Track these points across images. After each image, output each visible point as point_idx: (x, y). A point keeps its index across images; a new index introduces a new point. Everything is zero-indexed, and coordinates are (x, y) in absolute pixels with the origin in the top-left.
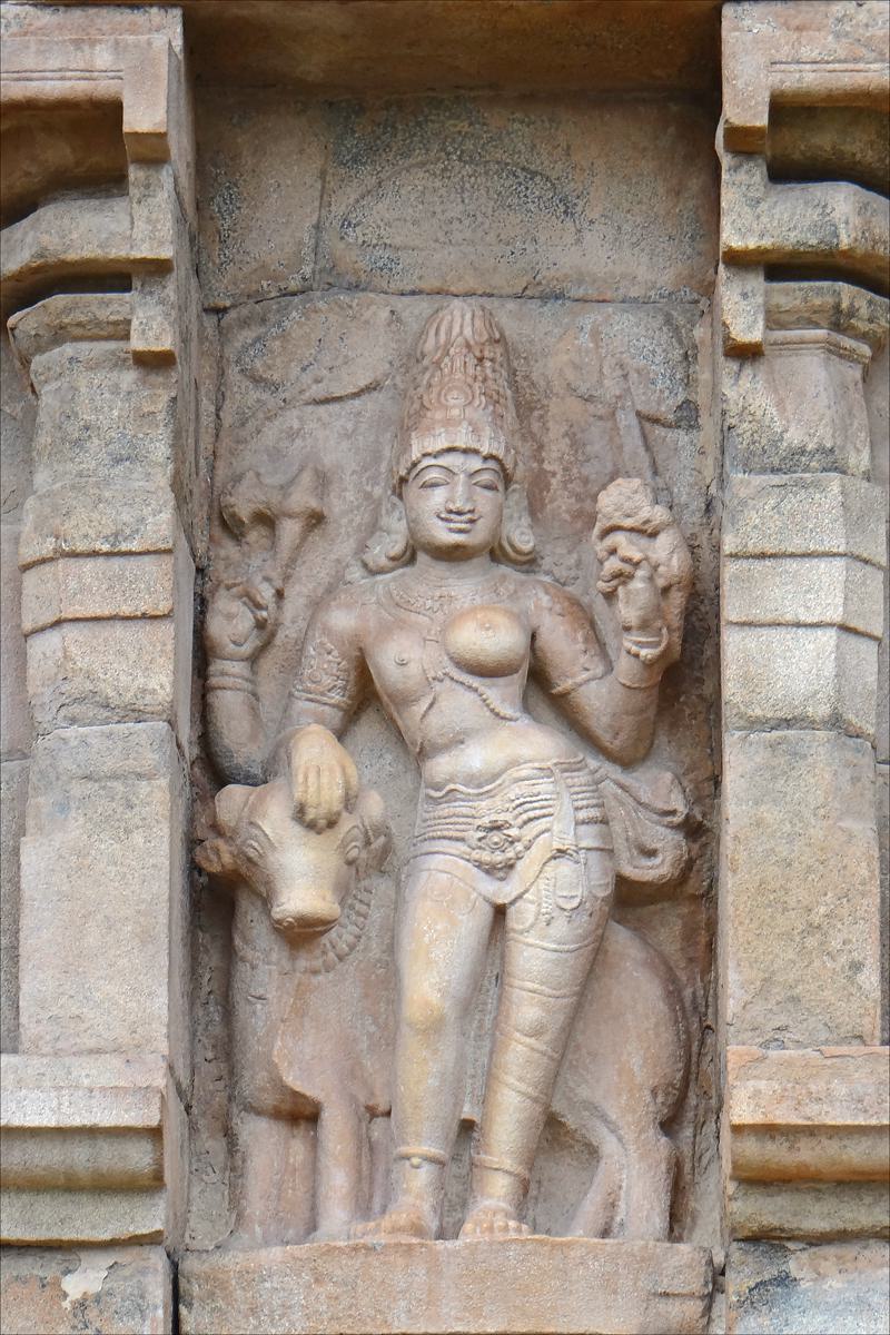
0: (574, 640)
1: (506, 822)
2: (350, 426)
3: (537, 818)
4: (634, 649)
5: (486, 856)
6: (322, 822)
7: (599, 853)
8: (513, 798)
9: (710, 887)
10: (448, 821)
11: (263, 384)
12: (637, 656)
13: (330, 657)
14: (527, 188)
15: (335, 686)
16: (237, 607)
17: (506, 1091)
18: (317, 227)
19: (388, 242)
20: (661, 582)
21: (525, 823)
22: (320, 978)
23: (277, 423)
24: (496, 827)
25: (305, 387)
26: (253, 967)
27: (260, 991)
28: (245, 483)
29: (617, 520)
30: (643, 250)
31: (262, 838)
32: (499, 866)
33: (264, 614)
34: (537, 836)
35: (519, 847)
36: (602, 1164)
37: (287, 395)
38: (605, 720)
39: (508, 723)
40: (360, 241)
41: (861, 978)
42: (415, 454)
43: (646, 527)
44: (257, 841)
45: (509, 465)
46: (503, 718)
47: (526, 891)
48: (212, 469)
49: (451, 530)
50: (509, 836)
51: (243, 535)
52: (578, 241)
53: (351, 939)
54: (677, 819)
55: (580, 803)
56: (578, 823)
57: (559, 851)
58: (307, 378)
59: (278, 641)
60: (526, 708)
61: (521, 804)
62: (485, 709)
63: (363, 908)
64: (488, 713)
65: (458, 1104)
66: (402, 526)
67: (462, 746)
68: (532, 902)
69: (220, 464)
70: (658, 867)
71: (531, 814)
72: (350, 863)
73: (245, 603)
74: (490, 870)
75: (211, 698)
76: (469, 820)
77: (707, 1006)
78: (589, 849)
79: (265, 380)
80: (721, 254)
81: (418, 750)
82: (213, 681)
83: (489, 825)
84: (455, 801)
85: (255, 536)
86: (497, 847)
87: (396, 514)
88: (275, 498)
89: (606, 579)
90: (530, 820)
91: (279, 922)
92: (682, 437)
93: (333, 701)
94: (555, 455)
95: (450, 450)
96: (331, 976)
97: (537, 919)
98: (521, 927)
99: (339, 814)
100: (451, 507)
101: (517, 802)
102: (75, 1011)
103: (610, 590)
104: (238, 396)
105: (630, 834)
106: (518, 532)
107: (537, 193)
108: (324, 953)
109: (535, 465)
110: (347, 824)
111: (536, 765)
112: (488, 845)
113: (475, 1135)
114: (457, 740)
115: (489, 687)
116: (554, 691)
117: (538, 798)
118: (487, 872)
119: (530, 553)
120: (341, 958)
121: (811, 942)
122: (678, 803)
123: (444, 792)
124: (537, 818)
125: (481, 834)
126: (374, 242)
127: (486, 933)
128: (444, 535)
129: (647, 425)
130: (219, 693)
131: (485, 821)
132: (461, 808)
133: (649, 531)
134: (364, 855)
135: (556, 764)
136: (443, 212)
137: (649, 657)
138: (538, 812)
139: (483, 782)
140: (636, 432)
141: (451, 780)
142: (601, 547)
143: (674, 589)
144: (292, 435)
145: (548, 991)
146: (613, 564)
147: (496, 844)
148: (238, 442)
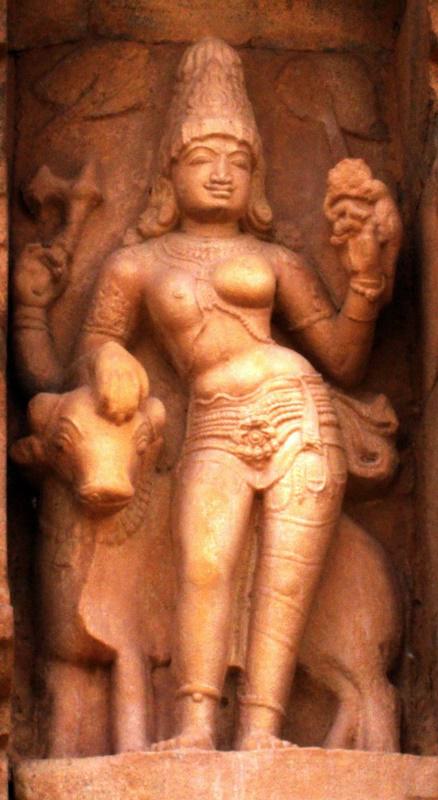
1: (265, 422)
3: (288, 419)
4: (361, 289)
5: (248, 450)
6: (122, 416)
10: (216, 422)
12: (363, 294)
16: (37, 266)
24: (256, 426)
29: (345, 189)
32: (259, 458)
33: (59, 269)
34: (290, 433)
35: (274, 442)
43: (366, 196)
46: (260, 341)
47: (283, 477)
49: (215, 196)
50: (267, 433)
53: (138, 520)
54: (390, 430)
55: (322, 409)
59: (67, 294)
61: (275, 409)
62: (246, 333)
64: (248, 337)
67: (227, 363)
70: (378, 466)
71: (284, 416)
76: (234, 421)
86: (255, 443)
87: (165, 192)
90: (284, 421)
93: (119, 333)
97: (291, 499)
99: (134, 410)
100: (215, 177)
101: (273, 406)
103: (340, 242)
112: (250, 442)
114: (224, 358)
122: (390, 417)
124: (288, 419)
125: (243, 432)
128: (207, 199)
129: (348, 138)
131: (248, 421)
133: (370, 198)
138: (289, 415)
139: (242, 393)
143: (389, 244)
146: (347, 221)
147: (256, 440)
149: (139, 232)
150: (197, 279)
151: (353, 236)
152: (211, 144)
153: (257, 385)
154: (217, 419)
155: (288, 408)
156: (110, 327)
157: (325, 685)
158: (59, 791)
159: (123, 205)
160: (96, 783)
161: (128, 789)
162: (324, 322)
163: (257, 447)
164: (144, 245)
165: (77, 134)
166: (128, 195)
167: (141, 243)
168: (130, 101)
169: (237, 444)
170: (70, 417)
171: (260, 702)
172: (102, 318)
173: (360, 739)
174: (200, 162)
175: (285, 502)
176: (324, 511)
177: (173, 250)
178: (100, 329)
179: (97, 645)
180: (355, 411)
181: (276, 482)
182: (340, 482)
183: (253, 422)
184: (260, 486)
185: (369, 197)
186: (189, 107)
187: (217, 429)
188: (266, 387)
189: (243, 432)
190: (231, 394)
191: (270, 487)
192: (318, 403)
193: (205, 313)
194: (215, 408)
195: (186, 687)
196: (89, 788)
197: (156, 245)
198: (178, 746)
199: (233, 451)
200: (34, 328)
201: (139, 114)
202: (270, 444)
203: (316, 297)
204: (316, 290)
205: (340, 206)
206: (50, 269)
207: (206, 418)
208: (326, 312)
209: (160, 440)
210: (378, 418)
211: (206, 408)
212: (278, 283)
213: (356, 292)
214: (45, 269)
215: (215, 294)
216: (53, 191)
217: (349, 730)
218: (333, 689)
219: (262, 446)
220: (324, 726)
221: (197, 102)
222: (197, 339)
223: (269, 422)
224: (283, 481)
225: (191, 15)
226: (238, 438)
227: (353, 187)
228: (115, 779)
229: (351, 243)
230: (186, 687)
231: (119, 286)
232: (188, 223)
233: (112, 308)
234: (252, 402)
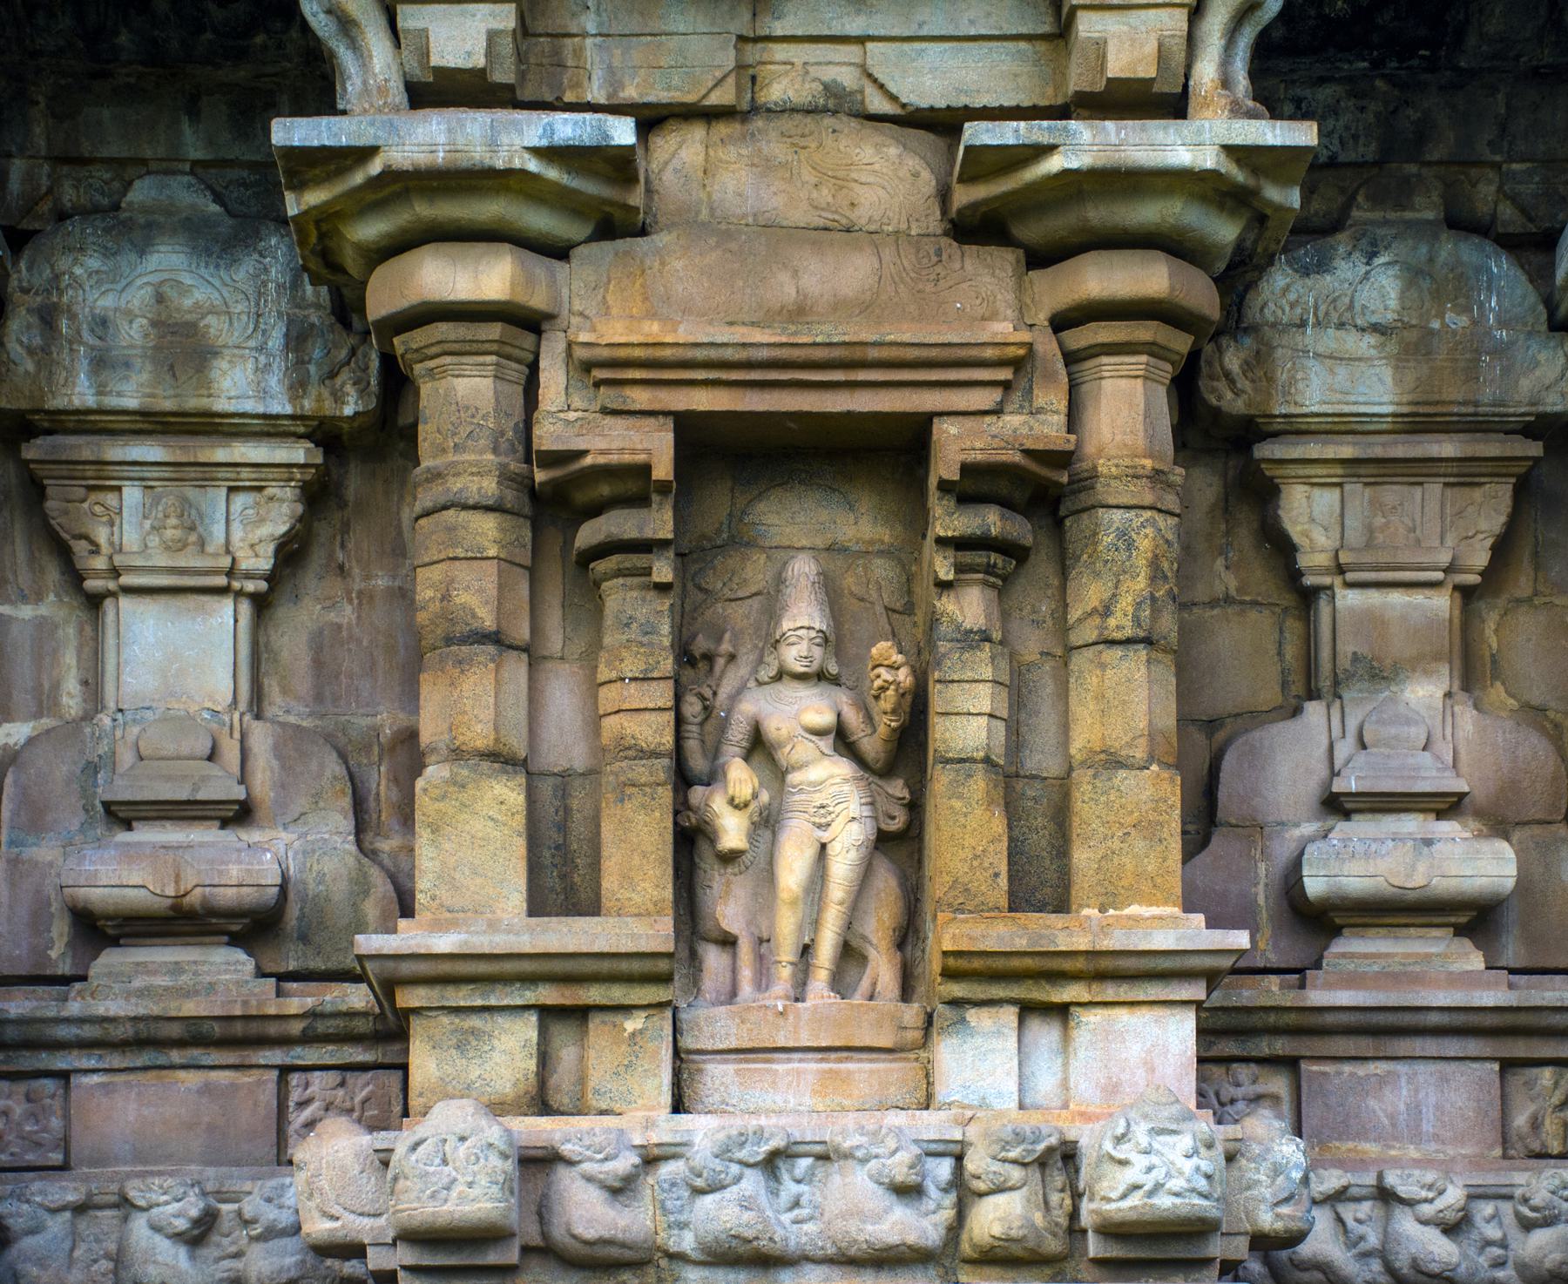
5: (817, 820)
41: (999, 880)
56: (862, 805)
58: (726, 590)
85: (700, 665)
86: (824, 816)
102: (628, 895)
121: (975, 863)
122: (906, 794)
131: (818, 804)
132: (803, 797)
139: (817, 785)
149: (757, 680)
168: (754, 589)
205: (877, 671)
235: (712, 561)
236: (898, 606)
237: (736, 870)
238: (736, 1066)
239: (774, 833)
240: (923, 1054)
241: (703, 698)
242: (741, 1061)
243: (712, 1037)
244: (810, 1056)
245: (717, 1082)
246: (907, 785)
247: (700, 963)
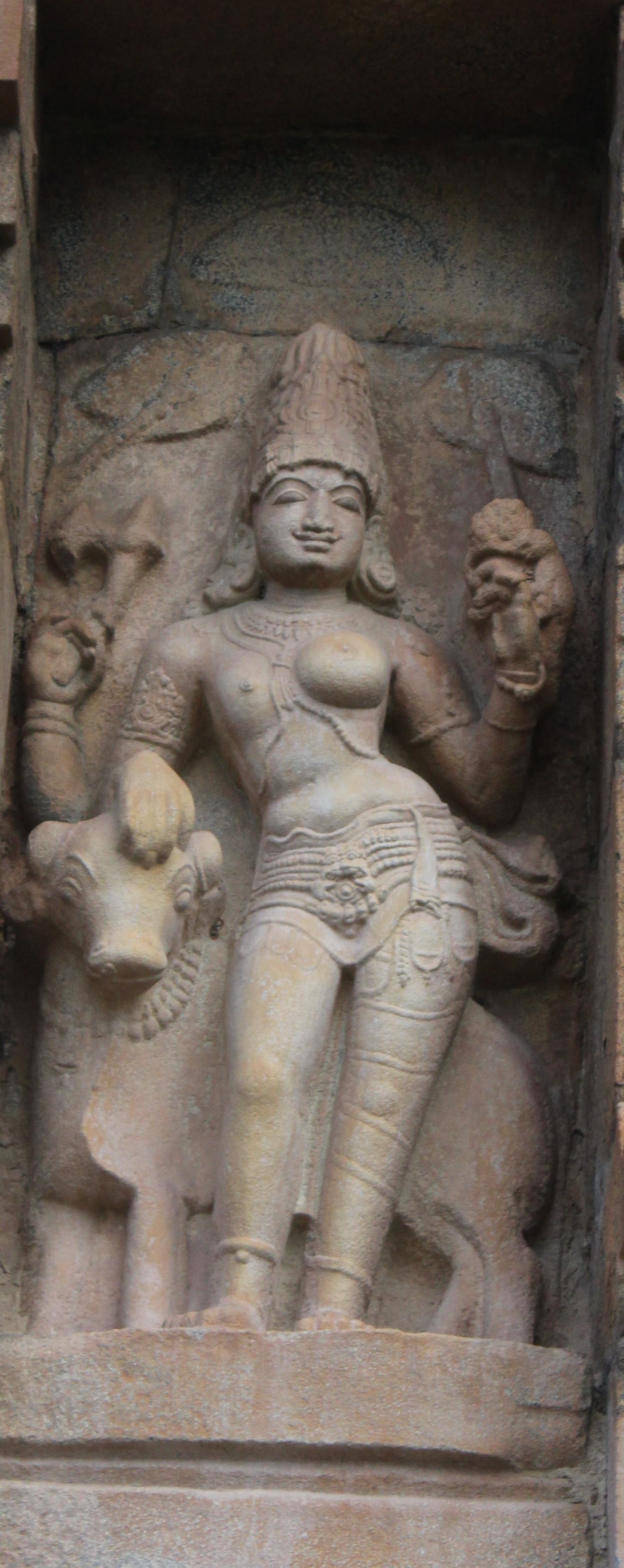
0: (439, 684)
1: (360, 870)
2: (193, 465)
3: (393, 867)
4: (509, 684)
5: (334, 909)
6: (153, 855)
7: (463, 911)
8: (368, 842)
9: (583, 970)
10: (292, 868)
11: (100, 420)
12: (511, 692)
13: (166, 691)
14: (394, 231)
15: (168, 724)
16: (61, 644)
17: (349, 1179)
18: (166, 263)
19: (242, 280)
20: (540, 613)
21: (381, 871)
22: (140, 1045)
23: (114, 460)
24: (348, 876)
25: (146, 422)
26: (63, 1032)
27: (70, 1058)
28: (77, 516)
29: (494, 542)
30: (517, 297)
31: (82, 873)
32: (349, 920)
33: (92, 650)
34: (394, 886)
35: (373, 898)
36: (456, 1275)
37: (128, 431)
38: (470, 770)
39: (364, 761)
40: (212, 278)
42: (270, 467)
43: (523, 552)
44: (75, 878)
45: (373, 488)
47: (379, 948)
48: (41, 505)
49: (308, 549)
50: (362, 886)
51: (71, 573)
52: (448, 287)
53: (176, 1004)
54: (548, 887)
55: (443, 853)
56: (446, 875)
57: (420, 903)
58: (149, 415)
60: (382, 750)
61: (373, 852)
62: (339, 743)
63: (190, 971)
64: (342, 748)
65: (292, 1195)
66: (252, 554)
67: (311, 785)
68: (385, 961)
69: (50, 502)
70: (527, 938)
71: (388, 862)
72: (180, 909)
73: (71, 641)
74: (339, 925)
75: (28, 741)
77: (576, 1108)
78: (452, 905)
79: (103, 416)
80: (618, 242)
81: (260, 791)
82: (32, 723)
83: (339, 872)
84: (300, 847)
85: (82, 576)
87: (244, 543)
88: (110, 531)
89: (479, 604)
90: (387, 868)
91: (96, 969)
92: (559, 487)
93: (165, 741)
94: (418, 499)
95: (309, 463)
96: (151, 1044)
97: (390, 980)
98: (372, 990)
99: (169, 846)
100: (309, 522)
101: (373, 847)
103: (481, 617)
104: (72, 432)
105: (495, 900)
106: (378, 565)
107: (405, 236)
108: (145, 1016)
109: (396, 509)
110: (178, 860)
111: (396, 806)
112: (337, 896)
113: (311, 1234)
115: (343, 718)
116: (413, 740)
117: (396, 843)
118: (334, 928)
119: (391, 591)
120: (163, 1025)
122: (549, 868)
123: (289, 836)
124: (393, 867)
125: (330, 883)
126: (227, 280)
127: (331, 996)
129: (521, 474)
130: (39, 736)
131: (336, 868)
133: (528, 556)
134: (195, 906)
135: (418, 807)
136: (303, 252)
137: (526, 692)
138: (396, 860)
140: (508, 479)
141: (298, 823)
142: (473, 576)
143: (554, 621)
144: (130, 473)
145: (401, 1064)
146: (490, 588)
147: (346, 894)
148: (71, 478)
149: (206, 599)
150: (274, 666)
151: (500, 610)
152: (307, 474)
153: (350, 818)
154: (294, 864)
155: (394, 851)
156: (154, 732)
157: (434, 1245)
158: (23, 1380)
159: (192, 562)
160: (75, 1369)
161: (120, 1380)
162: (459, 731)
163: (348, 905)
164: (211, 616)
165: (134, 462)
166: (198, 549)
167: (205, 614)
168: (210, 417)
169: (321, 900)
170: (80, 856)
171: (334, 1267)
172: (145, 719)
173: (477, 1323)
174: (288, 501)
175: (380, 986)
176: (439, 997)
177: (249, 626)
178: (140, 735)
179: (106, 1177)
180: (498, 858)
181: (371, 955)
182: (467, 957)
183: (342, 869)
184: (348, 960)
185: (527, 553)
186: (281, 423)
187: (292, 879)
188: (361, 820)
189: (330, 883)
190: (314, 829)
191: (364, 962)
192: (438, 845)
193: (283, 713)
194: (291, 848)
195: (228, 1241)
196: (66, 1377)
197: (225, 615)
198: (199, 1321)
199: (313, 909)
200: (52, 732)
201: (223, 433)
202: (367, 900)
203: (450, 696)
204: (451, 684)
206: (79, 649)
207: (279, 861)
208: (465, 716)
209: (215, 892)
210: (529, 868)
211: (279, 849)
212: (394, 675)
213: (502, 688)
214: (72, 647)
215: (296, 687)
216: (94, 540)
217: (464, 1310)
218: (447, 1254)
219: (354, 904)
220: (432, 1304)
221: (293, 415)
222: (270, 749)
223: (366, 870)
224: (380, 953)
225: (308, 295)
226: (321, 892)
227: (505, 539)
228: (105, 1367)
229: (496, 619)
230: (228, 1241)
231: (167, 673)
232: (272, 588)
233: (157, 705)
234: (344, 841)
235: (119, 358)
236: (540, 458)
237: (138, 1028)
238: (106, 1489)
239: (232, 945)
240: (578, 1477)
241: (82, 640)
242: (118, 1477)
243: (49, 1409)
244: (296, 1471)
245: (55, 1526)
246: (554, 844)
247: (41, 1255)
